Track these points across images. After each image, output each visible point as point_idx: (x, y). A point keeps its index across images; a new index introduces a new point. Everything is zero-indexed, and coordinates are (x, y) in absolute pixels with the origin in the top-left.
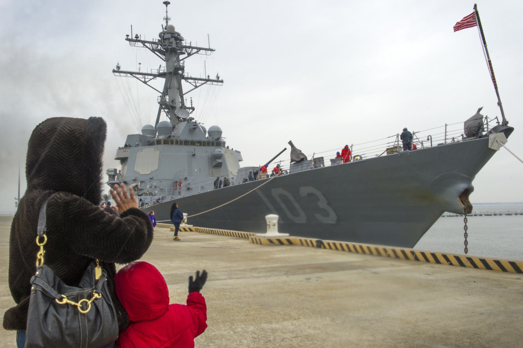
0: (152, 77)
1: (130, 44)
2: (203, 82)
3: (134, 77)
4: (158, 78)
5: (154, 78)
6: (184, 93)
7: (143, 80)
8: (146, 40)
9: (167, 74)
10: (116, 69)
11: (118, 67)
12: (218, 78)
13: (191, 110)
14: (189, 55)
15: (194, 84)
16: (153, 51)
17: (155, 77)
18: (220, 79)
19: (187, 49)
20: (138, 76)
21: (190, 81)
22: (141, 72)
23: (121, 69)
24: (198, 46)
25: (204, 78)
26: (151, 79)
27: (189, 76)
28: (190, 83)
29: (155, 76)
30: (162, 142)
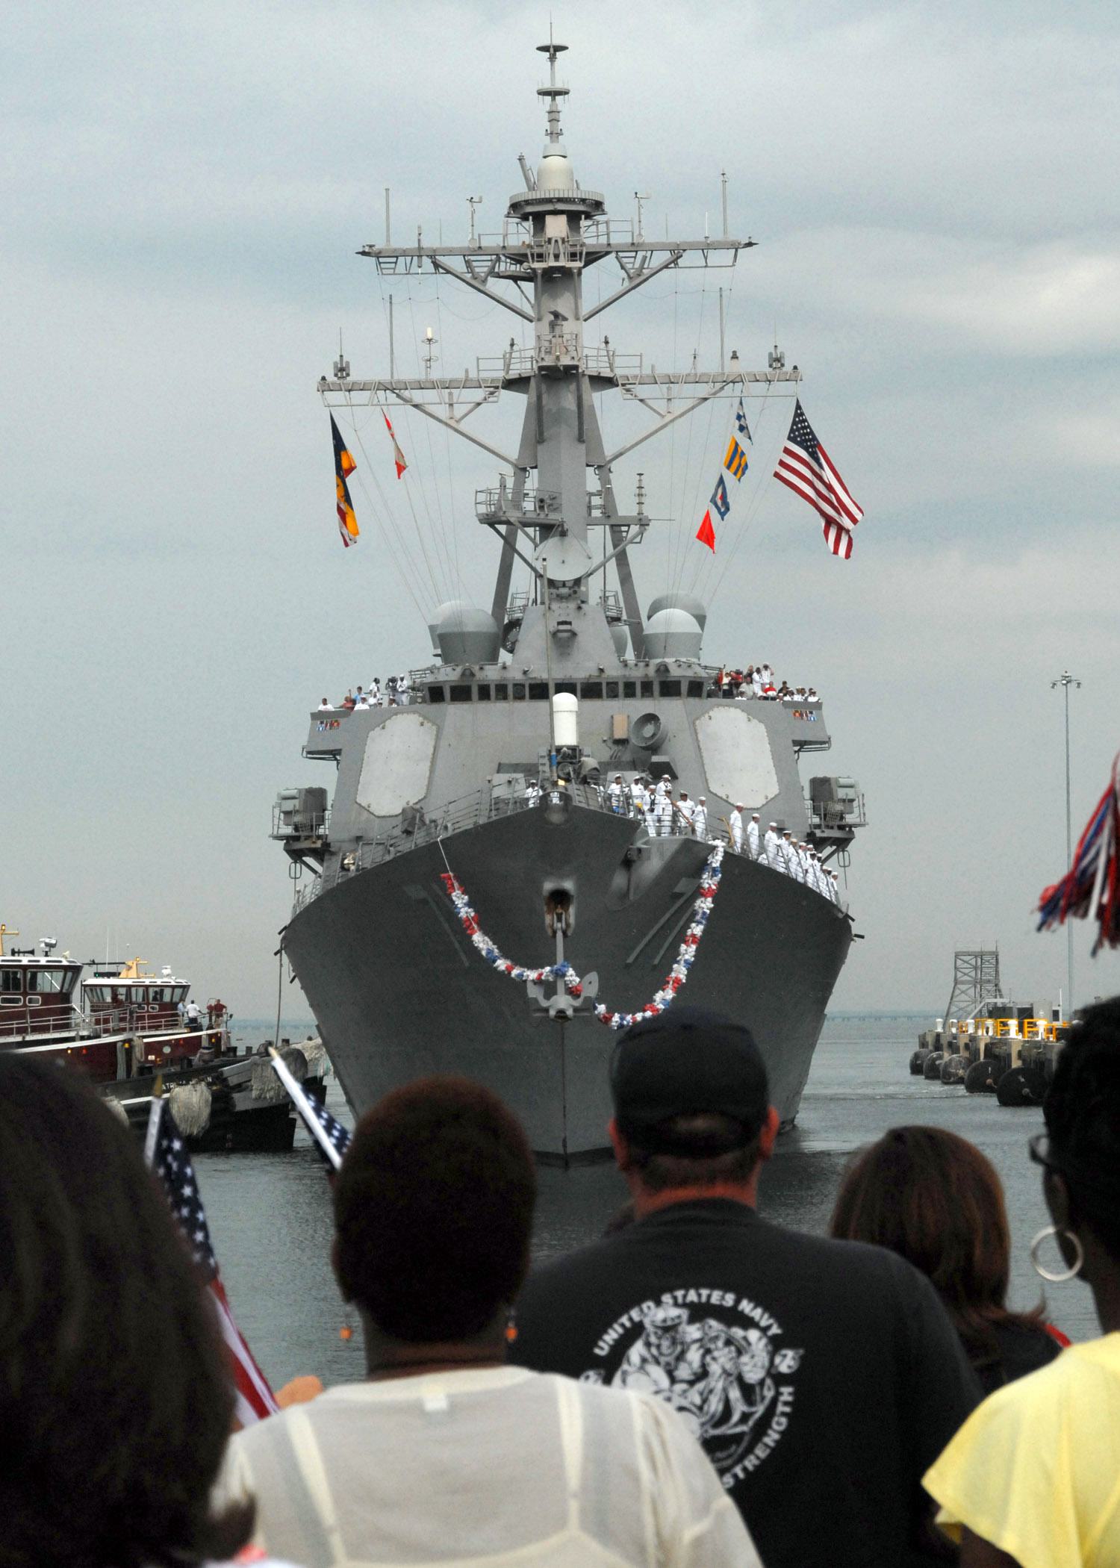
0: (479, 394)
1: (381, 269)
2: (703, 390)
3: (406, 401)
4: (504, 394)
5: (491, 399)
6: (609, 451)
7: (442, 412)
8: (444, 245)
9: (533, 383)
10: (331, 378)
11: (342, 370)
12: (776, 361)
13: (634, 529)
14: (637, 279)
15: (661, 406)
16: (477, 284)
17: (492, 393)
18: (788, 367)
19: (621, 254)
20: (417, 396)
21: (642, 391)
22: (435, 375)
23: (355, 376)
24: (675, 238)
25: (709, 365)
26: (479, 404)
27: (647, 371)
28: (641, 400)
29: (494, 388)
30: (447, 694)
